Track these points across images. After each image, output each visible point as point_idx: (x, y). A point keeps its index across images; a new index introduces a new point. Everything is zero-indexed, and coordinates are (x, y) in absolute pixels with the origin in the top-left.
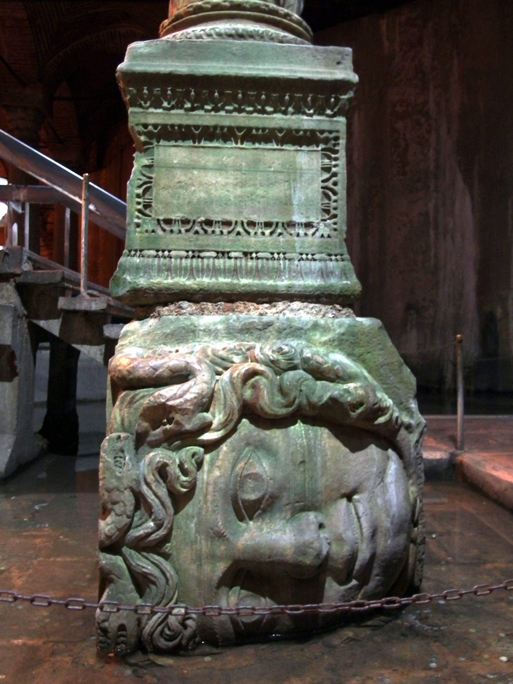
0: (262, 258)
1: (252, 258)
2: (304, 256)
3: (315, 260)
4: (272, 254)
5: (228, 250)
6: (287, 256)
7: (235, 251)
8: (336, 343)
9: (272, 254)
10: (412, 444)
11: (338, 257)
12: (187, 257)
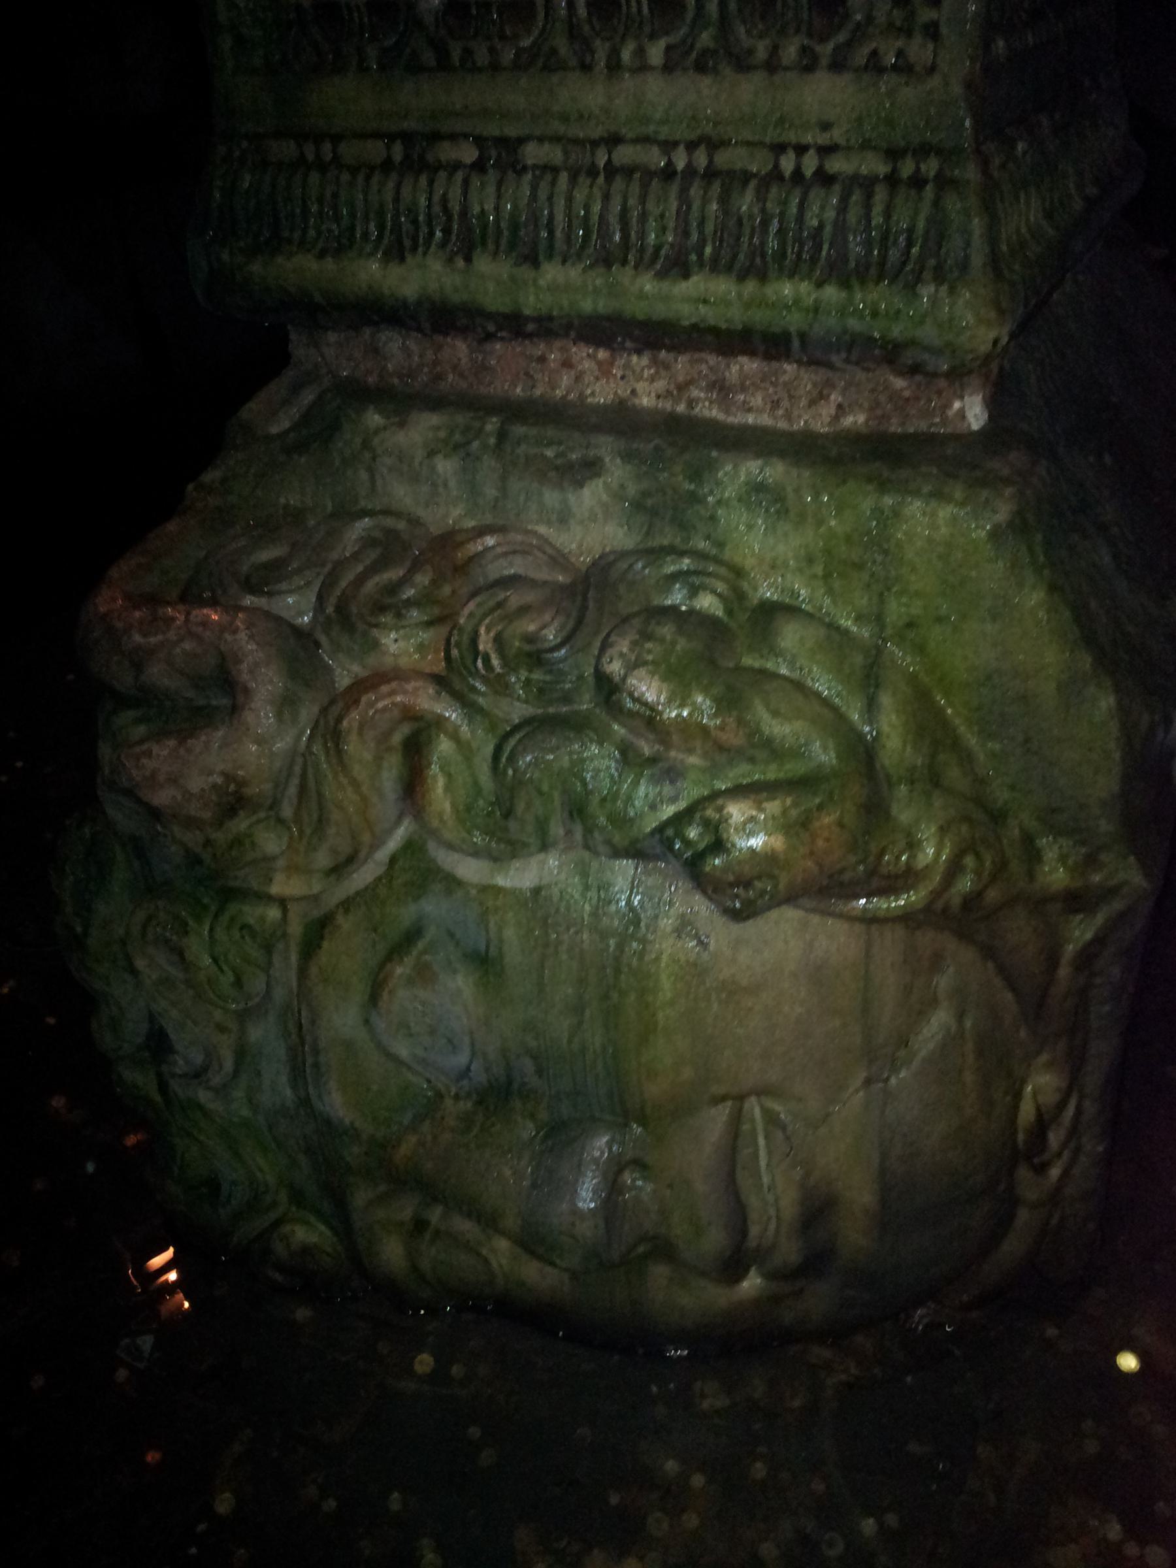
0: (629, 171)
1: (593, 172)
2: (787, 164)
3: (825, 179)
4: (668, 146)
5: (511, 131)
6: (723, 159)
7: (541, 140)
8: (819, 569)
9: (668, 146)
10: (1070, 949)
11: (931, 167)
12: (387, 165)
